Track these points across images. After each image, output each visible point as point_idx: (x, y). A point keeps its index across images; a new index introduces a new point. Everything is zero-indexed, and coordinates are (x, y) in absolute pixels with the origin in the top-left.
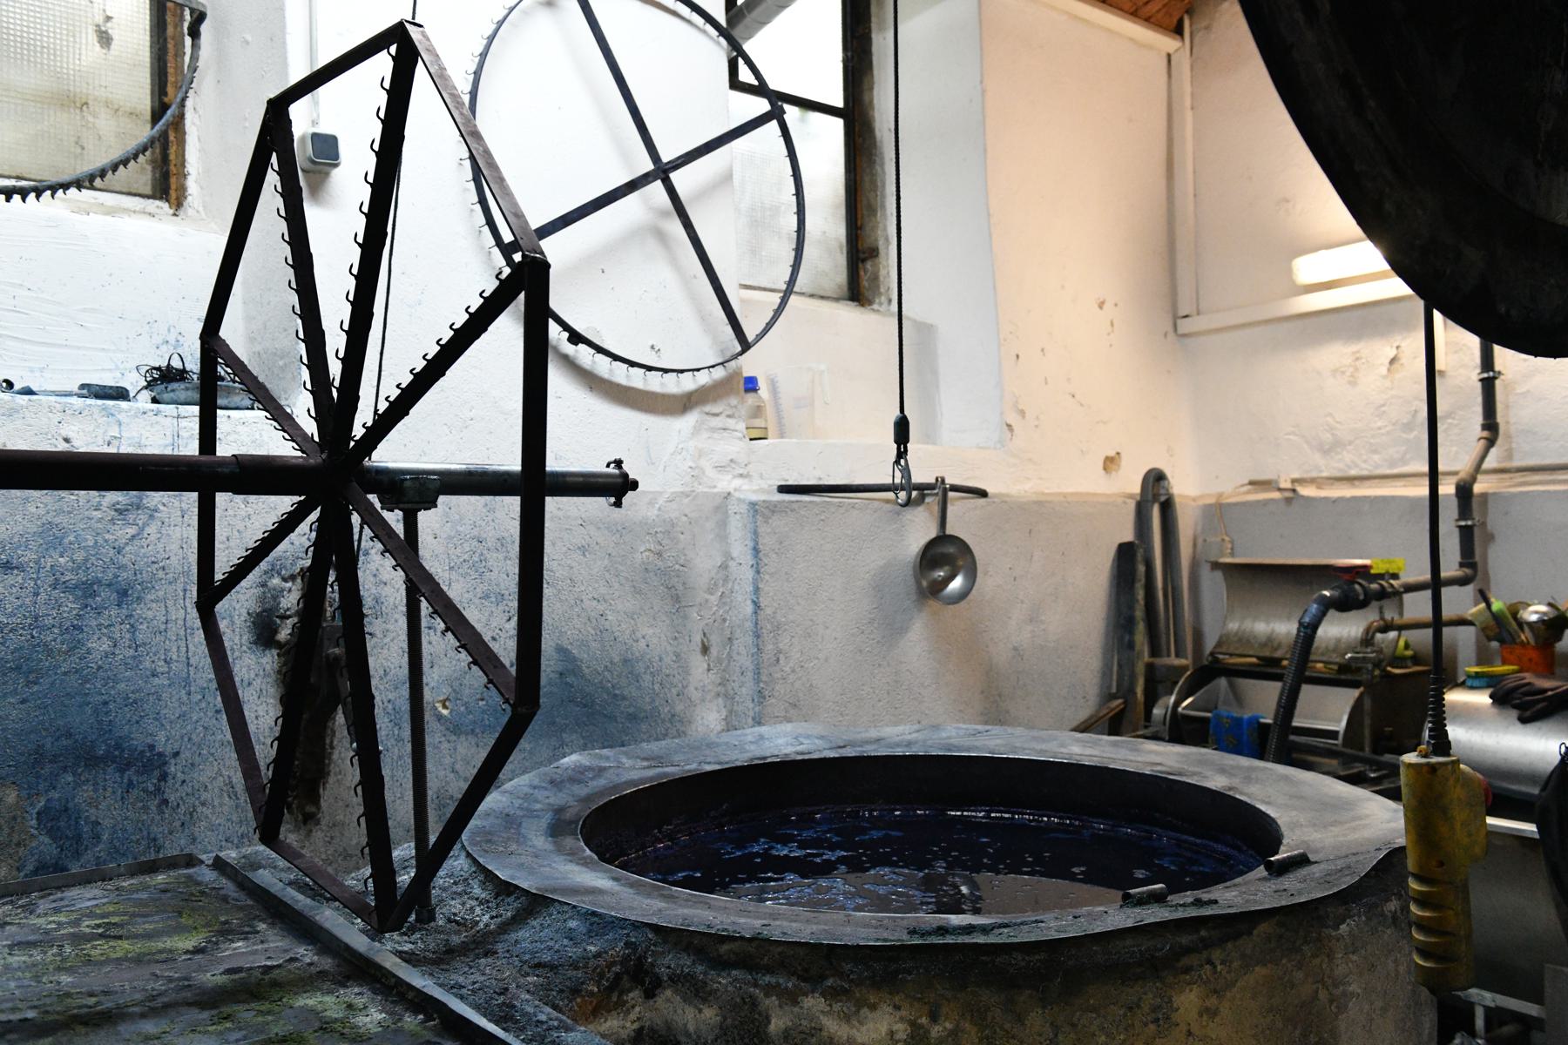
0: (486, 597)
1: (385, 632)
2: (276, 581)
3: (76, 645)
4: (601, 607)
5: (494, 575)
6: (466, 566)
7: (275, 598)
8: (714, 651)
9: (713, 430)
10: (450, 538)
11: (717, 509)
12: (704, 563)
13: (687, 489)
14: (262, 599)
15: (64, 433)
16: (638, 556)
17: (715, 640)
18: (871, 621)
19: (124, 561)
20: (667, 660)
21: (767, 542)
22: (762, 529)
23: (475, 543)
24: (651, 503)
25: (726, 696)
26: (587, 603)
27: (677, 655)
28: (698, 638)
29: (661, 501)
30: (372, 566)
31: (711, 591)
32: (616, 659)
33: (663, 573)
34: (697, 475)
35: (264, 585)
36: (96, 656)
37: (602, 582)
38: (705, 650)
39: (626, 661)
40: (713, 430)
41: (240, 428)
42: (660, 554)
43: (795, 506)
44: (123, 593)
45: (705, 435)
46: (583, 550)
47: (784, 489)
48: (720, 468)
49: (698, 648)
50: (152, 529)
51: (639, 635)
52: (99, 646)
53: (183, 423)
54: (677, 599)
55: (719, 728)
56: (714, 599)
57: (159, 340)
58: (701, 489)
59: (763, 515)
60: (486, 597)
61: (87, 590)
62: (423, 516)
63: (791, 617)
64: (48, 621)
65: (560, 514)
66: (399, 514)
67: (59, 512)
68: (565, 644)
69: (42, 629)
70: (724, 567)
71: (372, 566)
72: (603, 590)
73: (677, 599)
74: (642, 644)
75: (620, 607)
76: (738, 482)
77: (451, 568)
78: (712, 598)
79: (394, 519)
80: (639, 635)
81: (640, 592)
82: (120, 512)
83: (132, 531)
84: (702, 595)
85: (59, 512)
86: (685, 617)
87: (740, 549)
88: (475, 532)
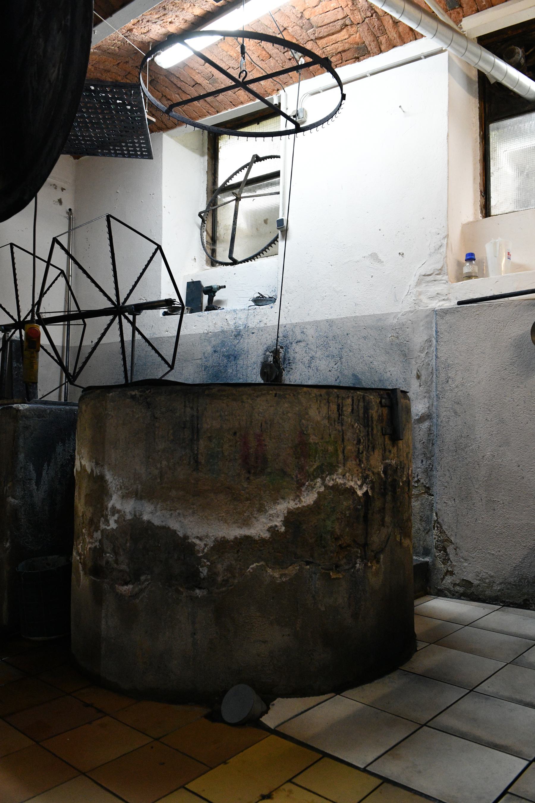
0: (328, 356)
1: (296, 368)
2: (268, 353)
3: (226, 370)
4: (371, 360)
5: (331, 349)
6: (322, 346)
7: (267, 358)
8: (423, 378)
9: (428, 282)
10: (317, 337)
11: (427, 316)
12: (419, 339)
13: (412, 309)
14: (264, 358)
15: (227, 318)
16: (388, 339)
17: (423, 373)
18: (512, 364)
19: (236, 349)
20: (400, 381)
21: (442, 328)
22: (440, 322)
23: (325, 338)
24: (395, 317)
25: (430, 397)
26: (365, 358)
27: (405, 379)
28: (415, 372)
29: (399, 316)
30: (293, 348)
31: (421, 351)
32: (377, 379)
33: (399, 345)
34: (417, 302)
35: (265, 354)
36: (229, 373)
37: (372, 350)
38: (418, 377)
39: (380, 381)
40: (428, 282)
41: (262, 311)
42: (397, 337)
43: (459, 309)
44: (235, 357)
45: (424, 285)
46: (365, 338)
47: (460, 303)
48: (432, 298)
49: (415, 377)
50: (241, 341)
51: (387, 370)
52: (230, 371)
53: (250, 311)
54: (405, 355)
55: (423, 411)
56: (423, 355)
57: (270, 290)
58: (420, 308)
59: (440, 316)
60: (328, 356)
61: (228, 357)
62: (137, 316)
63: (456, 362)
64: (221, 365)
65: (356, 325)
66: (132, 316)
67: (225, 337)
68: (356, 373)
69: (220, 366)
70: (429, 341)
71: (293, 348)
72: (372, 353)
73: (405, 355)
74: (389, 374)
75: (379, 359)
76: (441, 303)
77: (317, 347)
78: (422, 355)
79: (131, 317)
80: (387, 370)
81: (388, 353)
82: (236, 336)
83: (237, 341)
84: (417, 354)
85: (225, 337)
86: (409, 363)
87: (434, 333)
88: (325, 335)
